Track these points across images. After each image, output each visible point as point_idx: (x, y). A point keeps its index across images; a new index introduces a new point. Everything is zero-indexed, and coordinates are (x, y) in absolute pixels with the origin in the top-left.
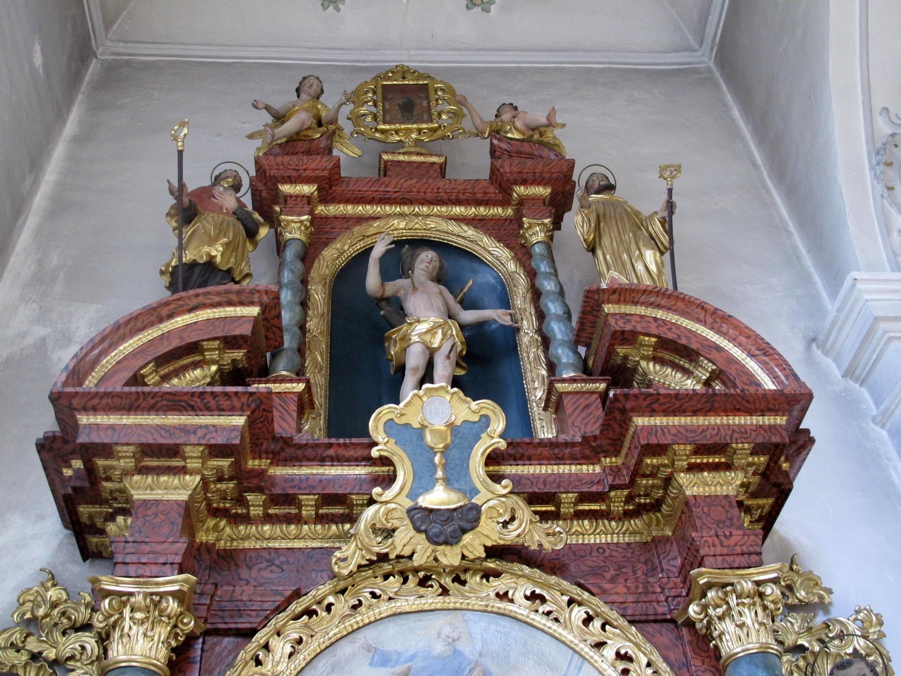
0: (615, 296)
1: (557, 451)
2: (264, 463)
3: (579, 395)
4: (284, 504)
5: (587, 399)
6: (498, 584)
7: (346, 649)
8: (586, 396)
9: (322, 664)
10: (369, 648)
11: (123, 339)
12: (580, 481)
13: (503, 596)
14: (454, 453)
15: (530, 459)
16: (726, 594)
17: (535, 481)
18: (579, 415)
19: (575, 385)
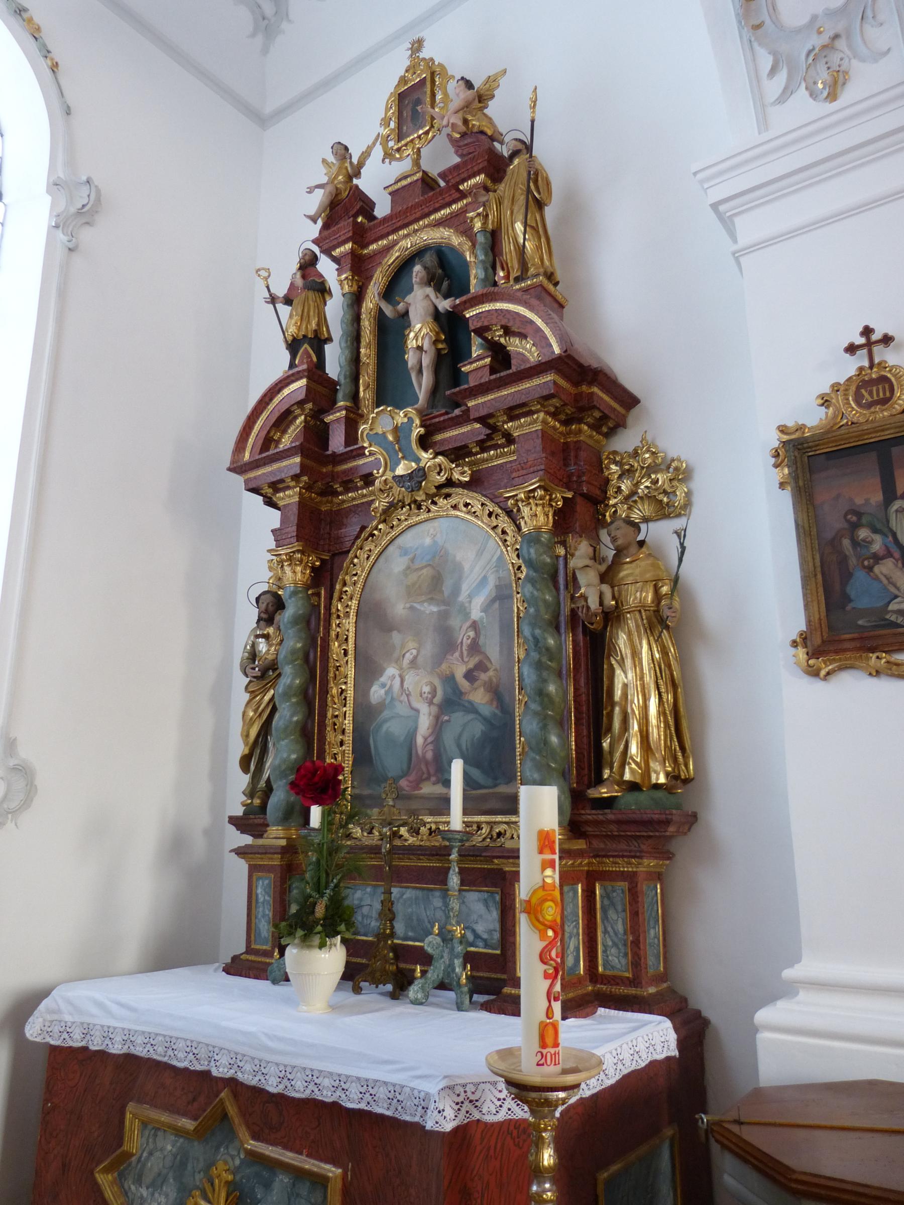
0: (468, 305)
2: (330, 468)
4: (348, 485)
6: (452, 501)
7: (391, 548)
9: (381, 560)
10: (400, 547)
11: (255, 422)
13: (455, 507)
14: (403, 442)
16: (517, 501)
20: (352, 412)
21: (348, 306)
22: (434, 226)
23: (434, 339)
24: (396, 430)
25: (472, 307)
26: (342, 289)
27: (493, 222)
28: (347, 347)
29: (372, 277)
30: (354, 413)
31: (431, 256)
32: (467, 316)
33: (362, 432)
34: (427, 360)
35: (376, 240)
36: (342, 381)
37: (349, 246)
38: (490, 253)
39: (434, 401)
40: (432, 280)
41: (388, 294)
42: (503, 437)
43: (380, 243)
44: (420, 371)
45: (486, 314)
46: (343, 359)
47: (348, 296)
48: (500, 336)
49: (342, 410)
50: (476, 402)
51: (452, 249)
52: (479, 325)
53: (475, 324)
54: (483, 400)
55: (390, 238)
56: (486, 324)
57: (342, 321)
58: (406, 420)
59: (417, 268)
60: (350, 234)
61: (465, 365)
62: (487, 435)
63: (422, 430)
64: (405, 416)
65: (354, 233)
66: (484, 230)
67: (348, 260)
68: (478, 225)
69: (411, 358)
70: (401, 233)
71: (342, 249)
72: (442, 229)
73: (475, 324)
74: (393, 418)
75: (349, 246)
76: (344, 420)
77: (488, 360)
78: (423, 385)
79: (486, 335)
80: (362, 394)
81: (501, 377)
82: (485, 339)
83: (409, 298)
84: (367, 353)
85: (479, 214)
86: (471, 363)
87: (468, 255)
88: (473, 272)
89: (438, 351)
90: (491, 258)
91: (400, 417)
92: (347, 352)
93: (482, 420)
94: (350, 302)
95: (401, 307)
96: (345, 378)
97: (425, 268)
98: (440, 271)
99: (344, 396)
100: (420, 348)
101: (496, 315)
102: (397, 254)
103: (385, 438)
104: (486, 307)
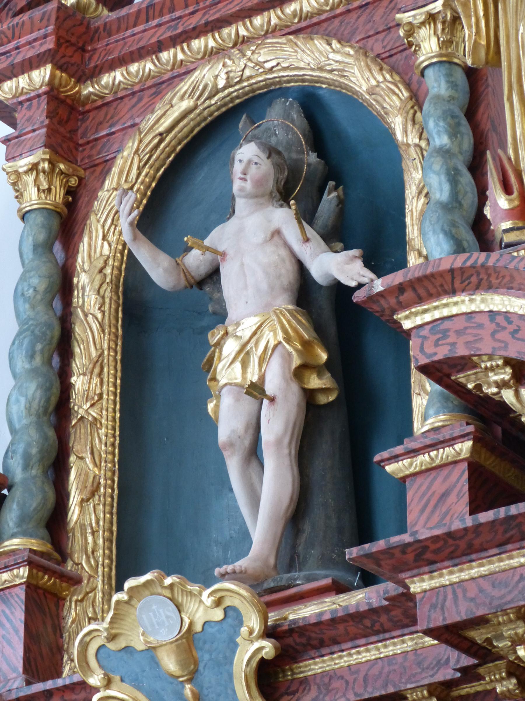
0: (408, 295)
1: (368, 622)
3: (434, 473)
5: (444, 480)
8: (445, 471)
12: (419, 664)
14: (207, 676)
15: (335, 642)
17: (350, 678)
18: (433, 512)
19: (421, 458)
20: (46, 570)
21: (36, 247)
22: (296, 32)
23: (296, 361)
24: (189, 642)
25: (420, 300)
26: (19, 196)
27: (476, 45)
28: (34, 372)
29: (106, 165)
30: (52, 573)
31: (287, 116)
32: (407, 325)
33: (84, 646)
34: (277, 425)
35: (123, 61)
36: (18, 474)
37: (41, 75)
38: (466, 128)
39: (294, 547)
40: (290, 188)
41: (158, 213)
42: (510, 674)
43: (134, 68)
44: (254, 453)
45: (460, 324)
46: (19, 408)
47: (38, 219)
48: (502, 385)
49: (17, 565)
50: (435, 583)
51: (351, 99)
52: (441, 353)
53: (429, 349)
54: (454, 578)
55: (165, 56)
56: (461, 351)
57: (18, 295)
58: (218, 614)
59: (247, 153)
60: (50, 44)
61: (395, 458)
62: (464, 670)
63: (268, 648)
64: (218, 603)
65: (59, 44)
66: (446, 62)
67: (39, 114)
68: (429, 45)
69: (228, 416)
70: (198, 44)
71: (23, 81)
72: (319, 43)
73: (429, 349)
74: (179, 608)
75: (41, 75)
76: (21, 593)
77: (465, 447)
78: (261, 498)
79: (461, 377)
80: (74, 513)
81: (509, 518)
82: (458, 390)
83: (220, 237)
84: (93, 388)
85: (432, 17)
86: (414, 452)
87: (397, 123)
88: (414, 177)
89: (309, 396)
90: (467, 142)
91: (202, 608)
92: (32, 388)
93: (452, 634)
94: (42, 237)
95: (195, 260)
96: (26, 467)
97: (271, 152)
98: (312, 158)
99: (22, 520)
100: (256, 390)
101: (490, 327)
102: (186, 104)
103: (155, 663)
104: (462, 304)
